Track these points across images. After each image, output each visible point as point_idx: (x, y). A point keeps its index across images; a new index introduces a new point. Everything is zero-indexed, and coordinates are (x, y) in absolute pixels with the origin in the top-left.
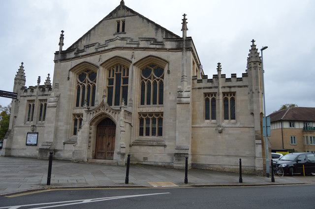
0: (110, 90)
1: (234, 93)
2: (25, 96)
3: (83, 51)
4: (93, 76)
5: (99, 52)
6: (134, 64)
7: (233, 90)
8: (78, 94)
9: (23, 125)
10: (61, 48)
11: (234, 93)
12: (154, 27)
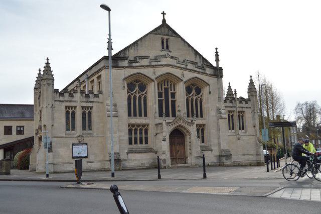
0: (160, 102)
1: (243, 112)
2: (62, 101)
3: (135, 61)
4: (143, 88)
5: (153, 66)
6: (185, 82)
7: (244, 109)
8: (129, 104)
9: (64, 135)
10: (110, 53)
11: (243, 112)
12: (194, 52)
